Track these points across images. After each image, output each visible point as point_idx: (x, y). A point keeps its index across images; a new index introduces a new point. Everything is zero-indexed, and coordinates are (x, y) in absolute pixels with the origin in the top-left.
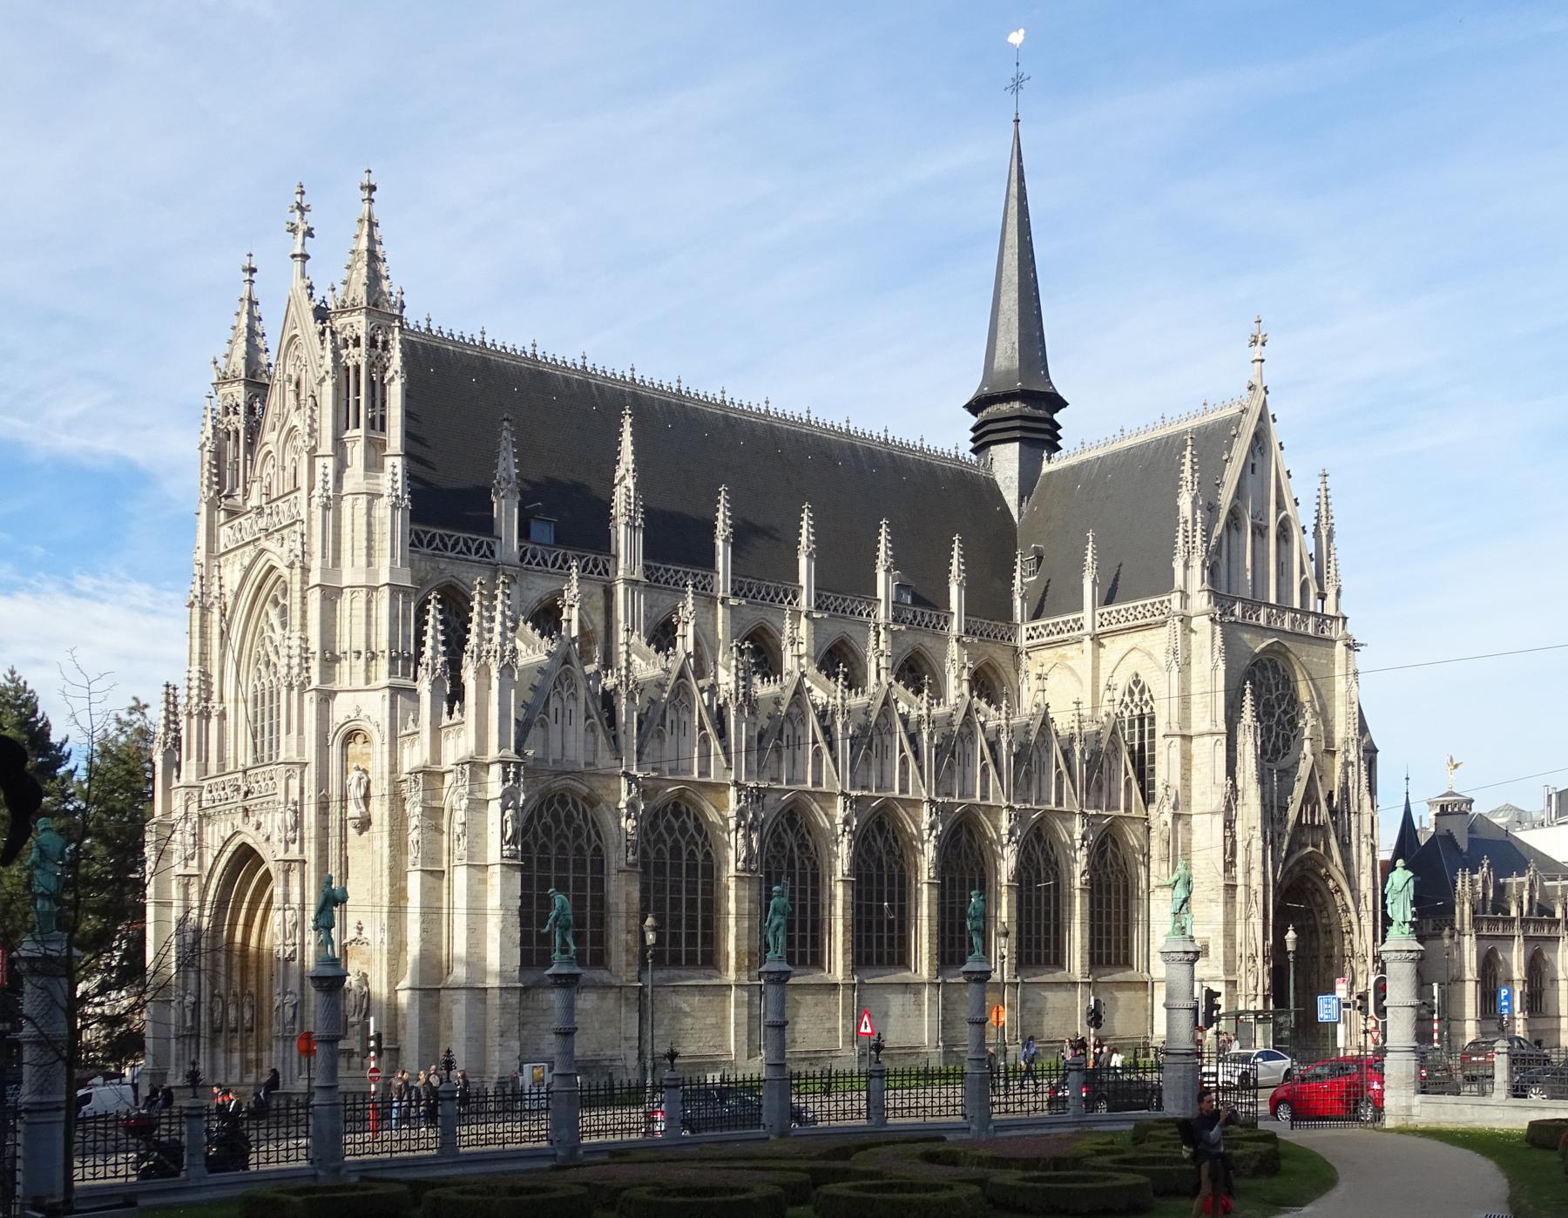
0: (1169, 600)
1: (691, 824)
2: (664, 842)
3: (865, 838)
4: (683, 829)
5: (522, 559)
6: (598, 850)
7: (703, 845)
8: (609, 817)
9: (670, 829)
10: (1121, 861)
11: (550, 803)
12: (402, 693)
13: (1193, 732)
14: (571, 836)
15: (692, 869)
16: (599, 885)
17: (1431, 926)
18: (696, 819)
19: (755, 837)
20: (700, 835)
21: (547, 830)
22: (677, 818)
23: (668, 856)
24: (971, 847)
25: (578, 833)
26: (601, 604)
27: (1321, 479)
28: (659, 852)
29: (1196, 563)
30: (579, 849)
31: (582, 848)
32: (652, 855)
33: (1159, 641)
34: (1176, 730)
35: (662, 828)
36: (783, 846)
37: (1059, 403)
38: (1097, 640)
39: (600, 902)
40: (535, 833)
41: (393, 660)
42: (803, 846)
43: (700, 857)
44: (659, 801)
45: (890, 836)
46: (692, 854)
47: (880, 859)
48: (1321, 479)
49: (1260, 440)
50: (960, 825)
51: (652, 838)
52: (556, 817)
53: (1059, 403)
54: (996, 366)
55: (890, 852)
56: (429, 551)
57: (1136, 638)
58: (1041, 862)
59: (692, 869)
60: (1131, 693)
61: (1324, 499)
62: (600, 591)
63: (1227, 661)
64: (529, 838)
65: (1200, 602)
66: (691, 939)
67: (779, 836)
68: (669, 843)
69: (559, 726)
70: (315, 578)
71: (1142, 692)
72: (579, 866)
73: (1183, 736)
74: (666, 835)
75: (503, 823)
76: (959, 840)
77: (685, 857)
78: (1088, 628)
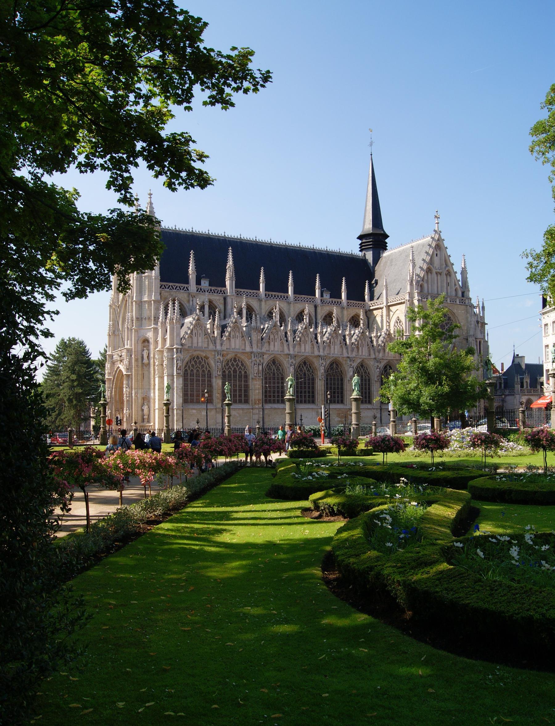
1: (240, 364)
2: (231, 369)
3: (299, 367)
4: (237, 365)
5: (197, 291)
6: (209, 371)
9: (233, 365)
11: (194, 358)
12: (156, 330)
15: (240, 377)
16: (210, 381)
18: (241, 362)
19: (260, 367)
21: (193, 366)
23: (232, 372)
25: (203, 366)
26: (223, 302)
28: (230, 372)
30: (203, 371)
32: (227, 372)
35: (230, 365)
36: (271, 369)
37: (387, 236)
38: (388, 307)
39: (210, 386)
40: (189, 366)
41: (154, 320)
42: (278, 369)
43: (243, 373)
44: (229, 357)
45: (309, 366)
46: (240, 372)
47: (305, 373)
51: (227, 367)
52: (195, 362)
53: (387, 236)
54: (365, 227)
55: (309, 371)
56: (168, 290)
59: (240, 377)
60: (397, 323)
62: (222, 299)
64: (187, 368)
66: (240, 396)
67: (270, 367)
68: (233, 369)
69: (196, 338)
70: (134, 299)
71: (400, 322)
72: (203, 376)
75: (177, 364)
77: (238, 372)
78: (385, 304)
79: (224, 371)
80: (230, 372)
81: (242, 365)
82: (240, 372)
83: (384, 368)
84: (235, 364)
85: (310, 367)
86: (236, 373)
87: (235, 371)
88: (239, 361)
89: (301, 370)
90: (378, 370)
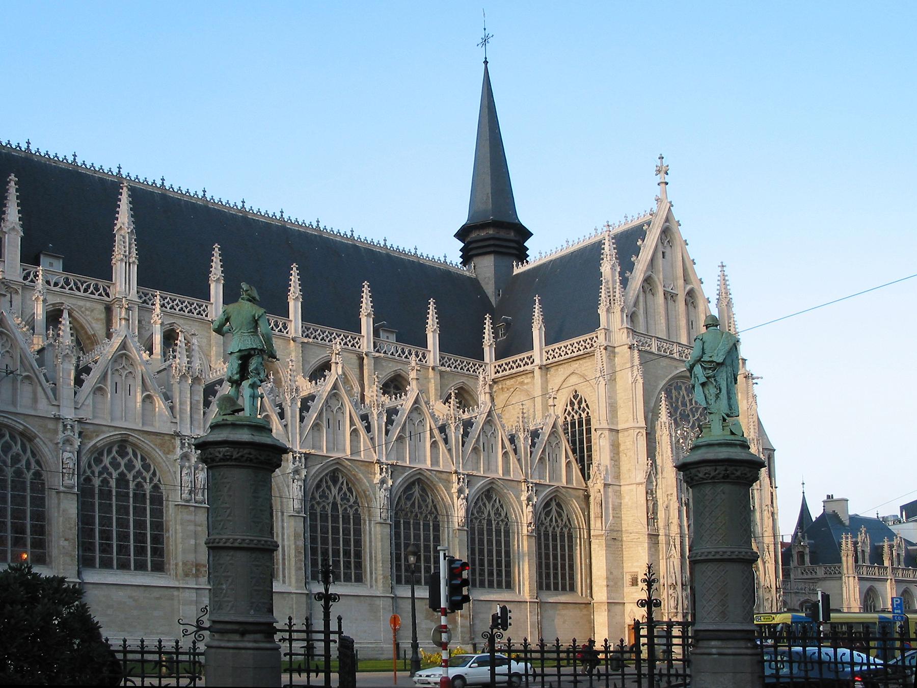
0: (597, 337)
1: (138, 464)
2: (110, 474)
3: (318, 486)
4: (130, 466)
7: (151, 480)
8: (46, 450)
9: (116, 465)
10: (565, 519)
13: (620, 427)
14: (9, 461)
17: (823, 573)
20: (148, 471)
22: (123, 457)
23: (113, 483)
24: (425, 501)
25: (16, 459)
27: (720, 269)
28: (105, 482)
29: (617, 308)
31: (22, 473)
33: (592, 368)
34: (605, 425)
43: (148, 487)
46: (139, 486)
47: (335, 505)
48: (720, 269)
49: (667, 233)
50: (413, 483)
51: (97, 470)
55: (345, 498)
57: (575, 365)
58: (492, 515)
61: (724, 281)
63: (644, 378)
65: (621, 338)
73: (611, 430)
74: (111, 469)
76: (412, 494)
79: (88, 480)
80: (105, 482)
81: (146, 467)
82: (139, 486)
83: (545, 507)
84: (123, 464)
85: (350, 490)
86: (127, 487)
87: (122, 481)
88: (135, 455)
89: (324, 496)
90: (530, 508)
